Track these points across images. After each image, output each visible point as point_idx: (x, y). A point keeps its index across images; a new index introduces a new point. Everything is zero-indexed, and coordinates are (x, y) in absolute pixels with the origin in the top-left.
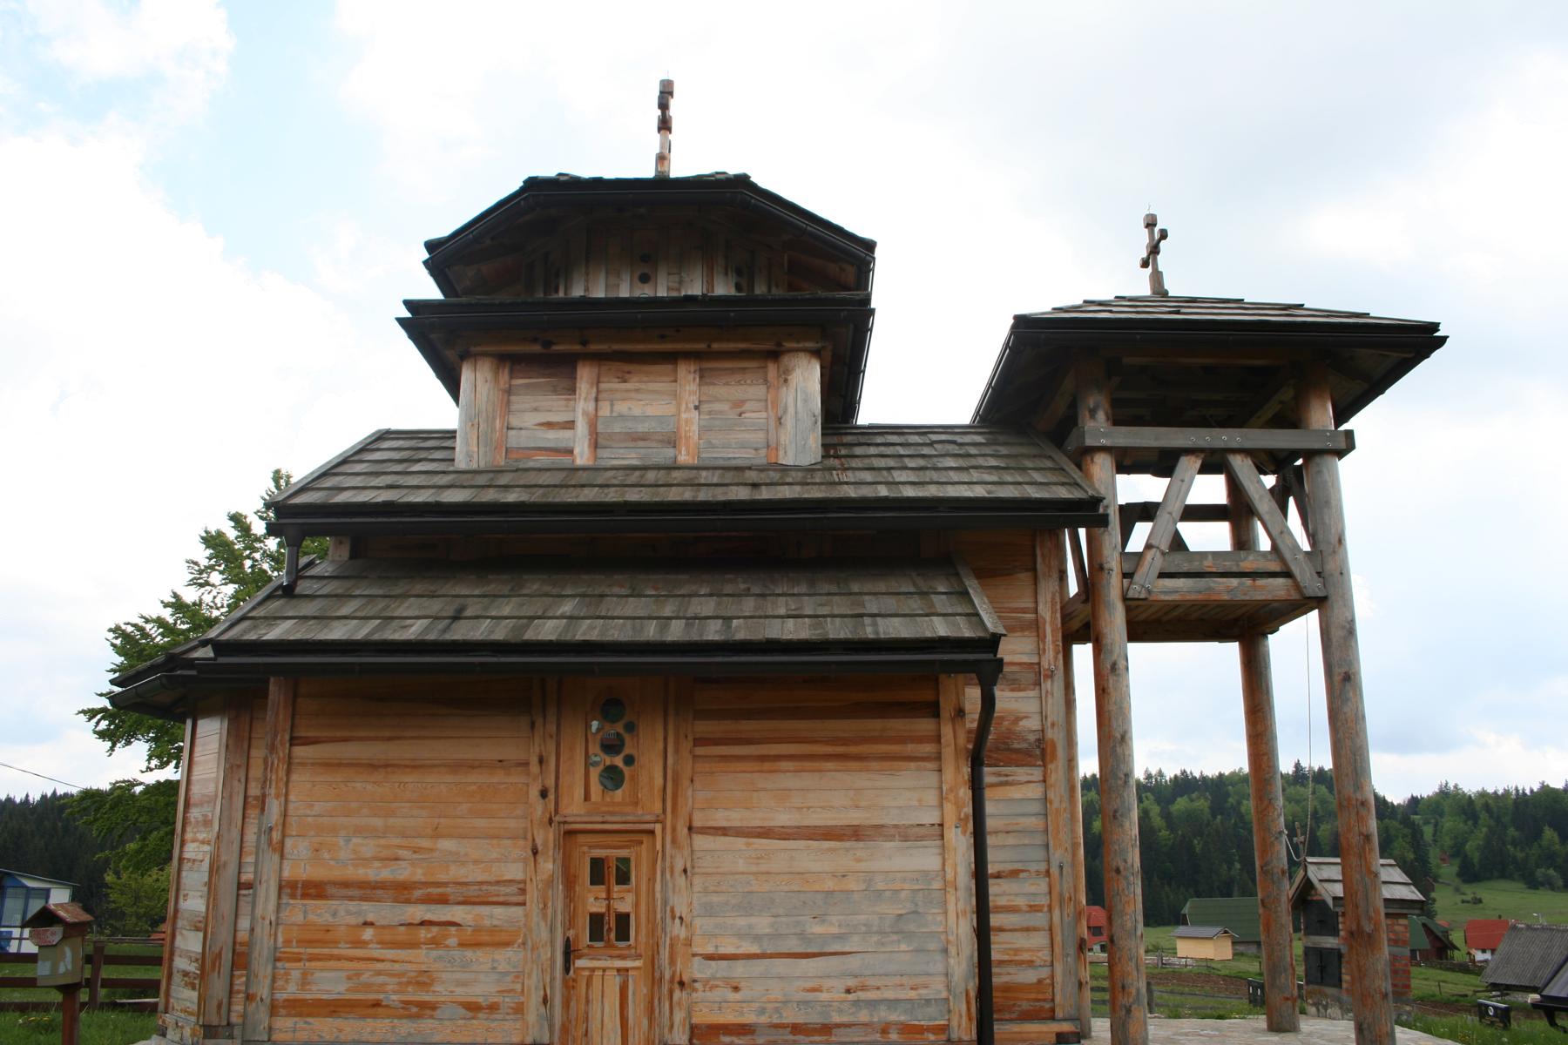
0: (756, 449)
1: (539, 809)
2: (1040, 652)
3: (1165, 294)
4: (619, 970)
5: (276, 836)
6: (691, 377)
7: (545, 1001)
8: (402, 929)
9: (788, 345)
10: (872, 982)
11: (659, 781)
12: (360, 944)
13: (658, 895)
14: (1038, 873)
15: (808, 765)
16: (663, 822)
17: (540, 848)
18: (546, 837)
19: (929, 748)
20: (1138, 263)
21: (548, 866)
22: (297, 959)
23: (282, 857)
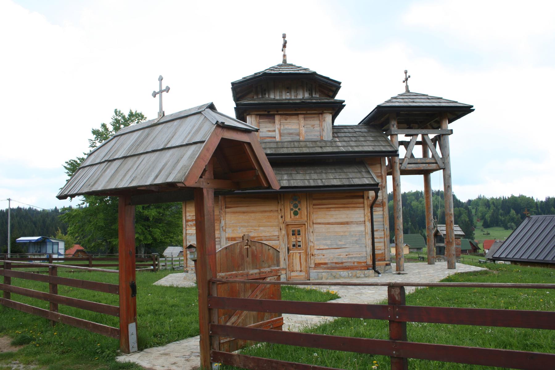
0: (318, 136)
1: (281, 220)
3: (409, 91)
4: (299, 253)
5: (224, 228)
6: (302, 119)
7: (285, 260)
9: (325, 112)
10: (351, 253)
13: (307, 237)
14: (382, 230)
15: (337, 209)
16: (307, 222)
17: (282, 228)
18: (283, 226)
19: (362, 205)
20: (402, 81)
21: (284, 232)
23: (226, 232)
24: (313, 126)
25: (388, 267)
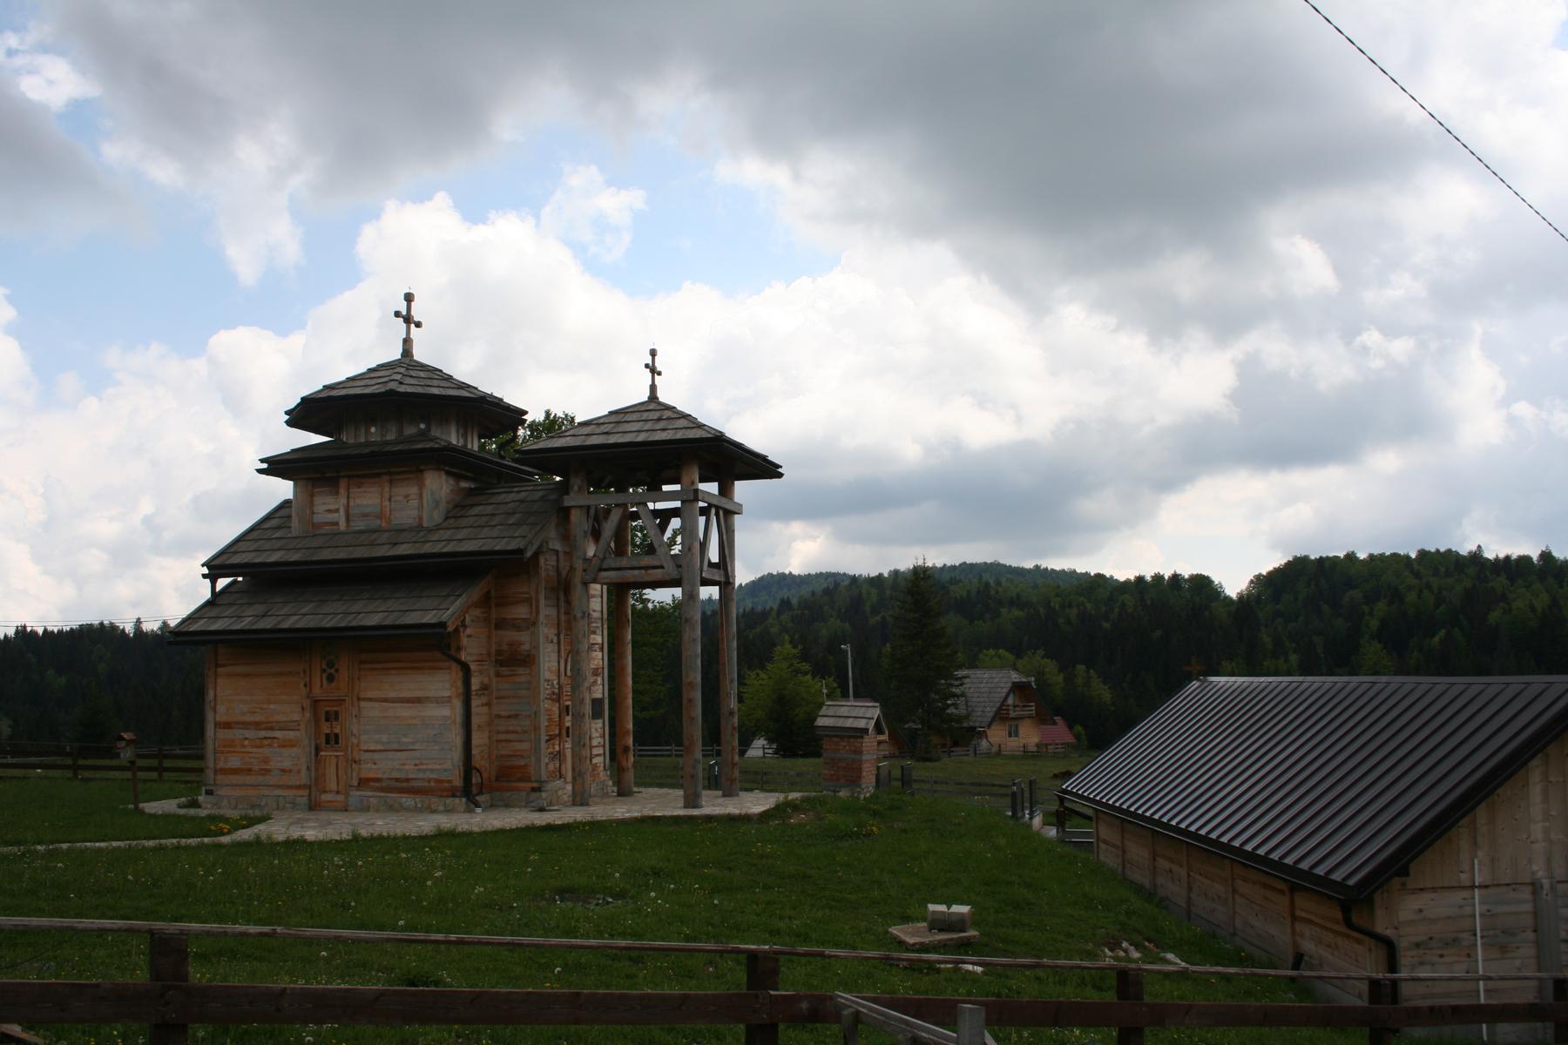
0: (414, 518)
1: (304, 691)
2: (531, 613)
6: (386, 483)
8: (258, 741)
11: (347, 679)
12: (244, 746)
18: (307, 703)
19: (447, 664)
21: (308, 715)
22: (222, 752)
23: (215, 712)
24: (406, 496)
25: (534, 795)
